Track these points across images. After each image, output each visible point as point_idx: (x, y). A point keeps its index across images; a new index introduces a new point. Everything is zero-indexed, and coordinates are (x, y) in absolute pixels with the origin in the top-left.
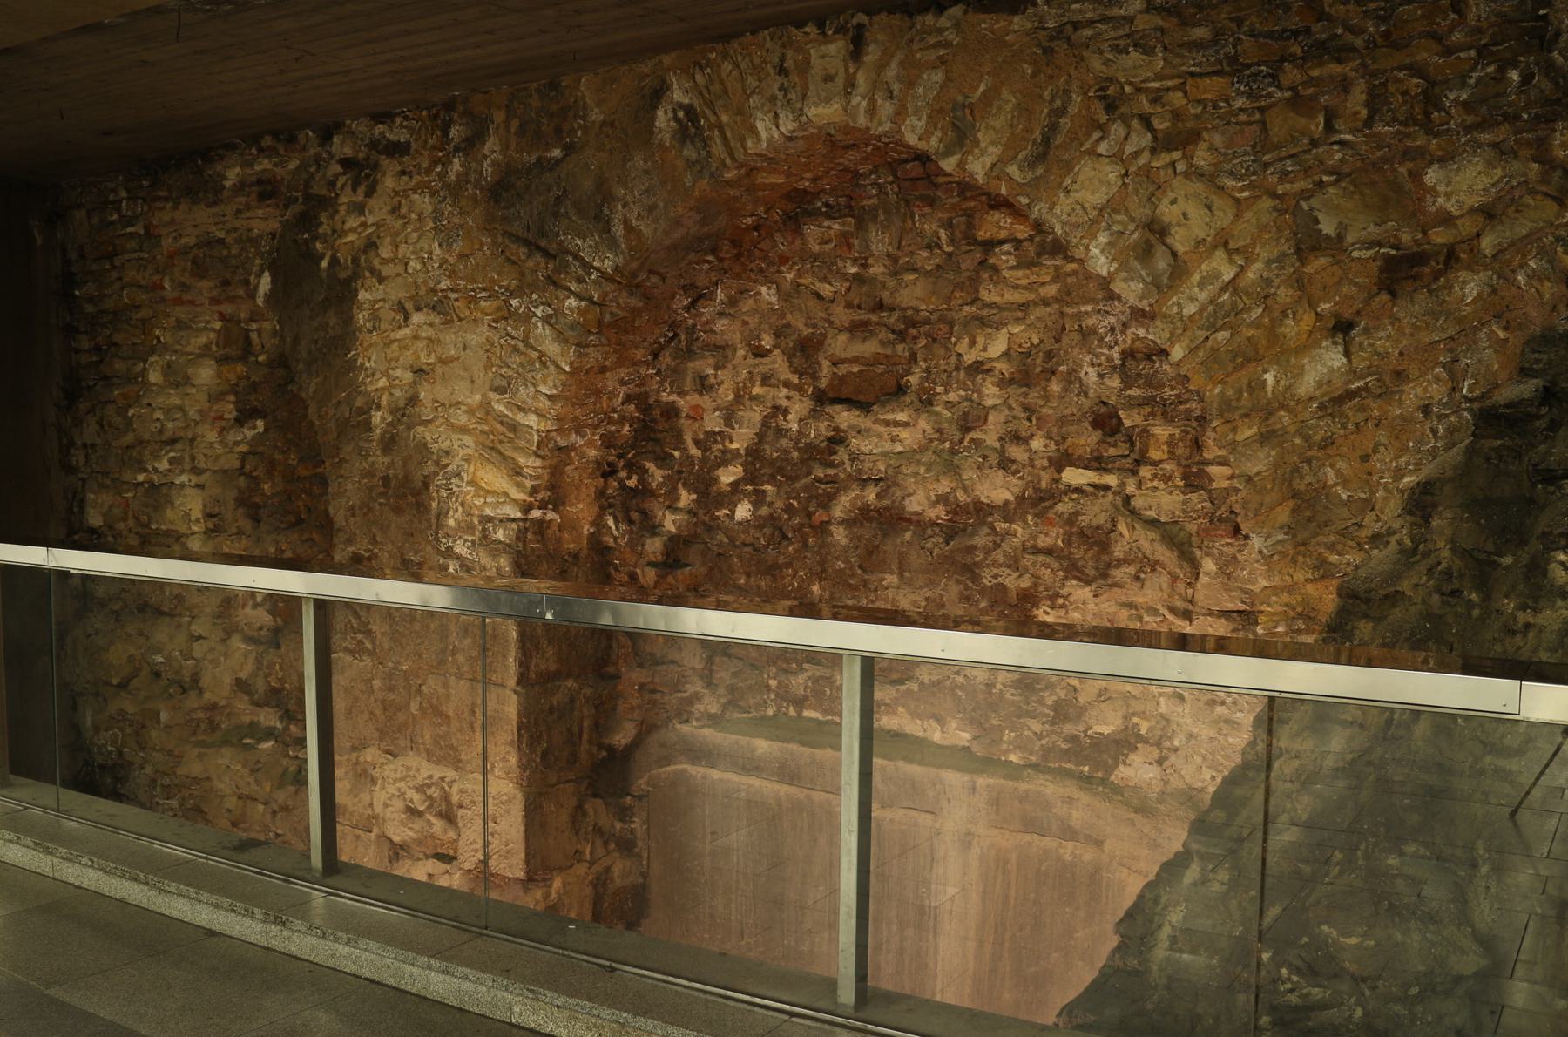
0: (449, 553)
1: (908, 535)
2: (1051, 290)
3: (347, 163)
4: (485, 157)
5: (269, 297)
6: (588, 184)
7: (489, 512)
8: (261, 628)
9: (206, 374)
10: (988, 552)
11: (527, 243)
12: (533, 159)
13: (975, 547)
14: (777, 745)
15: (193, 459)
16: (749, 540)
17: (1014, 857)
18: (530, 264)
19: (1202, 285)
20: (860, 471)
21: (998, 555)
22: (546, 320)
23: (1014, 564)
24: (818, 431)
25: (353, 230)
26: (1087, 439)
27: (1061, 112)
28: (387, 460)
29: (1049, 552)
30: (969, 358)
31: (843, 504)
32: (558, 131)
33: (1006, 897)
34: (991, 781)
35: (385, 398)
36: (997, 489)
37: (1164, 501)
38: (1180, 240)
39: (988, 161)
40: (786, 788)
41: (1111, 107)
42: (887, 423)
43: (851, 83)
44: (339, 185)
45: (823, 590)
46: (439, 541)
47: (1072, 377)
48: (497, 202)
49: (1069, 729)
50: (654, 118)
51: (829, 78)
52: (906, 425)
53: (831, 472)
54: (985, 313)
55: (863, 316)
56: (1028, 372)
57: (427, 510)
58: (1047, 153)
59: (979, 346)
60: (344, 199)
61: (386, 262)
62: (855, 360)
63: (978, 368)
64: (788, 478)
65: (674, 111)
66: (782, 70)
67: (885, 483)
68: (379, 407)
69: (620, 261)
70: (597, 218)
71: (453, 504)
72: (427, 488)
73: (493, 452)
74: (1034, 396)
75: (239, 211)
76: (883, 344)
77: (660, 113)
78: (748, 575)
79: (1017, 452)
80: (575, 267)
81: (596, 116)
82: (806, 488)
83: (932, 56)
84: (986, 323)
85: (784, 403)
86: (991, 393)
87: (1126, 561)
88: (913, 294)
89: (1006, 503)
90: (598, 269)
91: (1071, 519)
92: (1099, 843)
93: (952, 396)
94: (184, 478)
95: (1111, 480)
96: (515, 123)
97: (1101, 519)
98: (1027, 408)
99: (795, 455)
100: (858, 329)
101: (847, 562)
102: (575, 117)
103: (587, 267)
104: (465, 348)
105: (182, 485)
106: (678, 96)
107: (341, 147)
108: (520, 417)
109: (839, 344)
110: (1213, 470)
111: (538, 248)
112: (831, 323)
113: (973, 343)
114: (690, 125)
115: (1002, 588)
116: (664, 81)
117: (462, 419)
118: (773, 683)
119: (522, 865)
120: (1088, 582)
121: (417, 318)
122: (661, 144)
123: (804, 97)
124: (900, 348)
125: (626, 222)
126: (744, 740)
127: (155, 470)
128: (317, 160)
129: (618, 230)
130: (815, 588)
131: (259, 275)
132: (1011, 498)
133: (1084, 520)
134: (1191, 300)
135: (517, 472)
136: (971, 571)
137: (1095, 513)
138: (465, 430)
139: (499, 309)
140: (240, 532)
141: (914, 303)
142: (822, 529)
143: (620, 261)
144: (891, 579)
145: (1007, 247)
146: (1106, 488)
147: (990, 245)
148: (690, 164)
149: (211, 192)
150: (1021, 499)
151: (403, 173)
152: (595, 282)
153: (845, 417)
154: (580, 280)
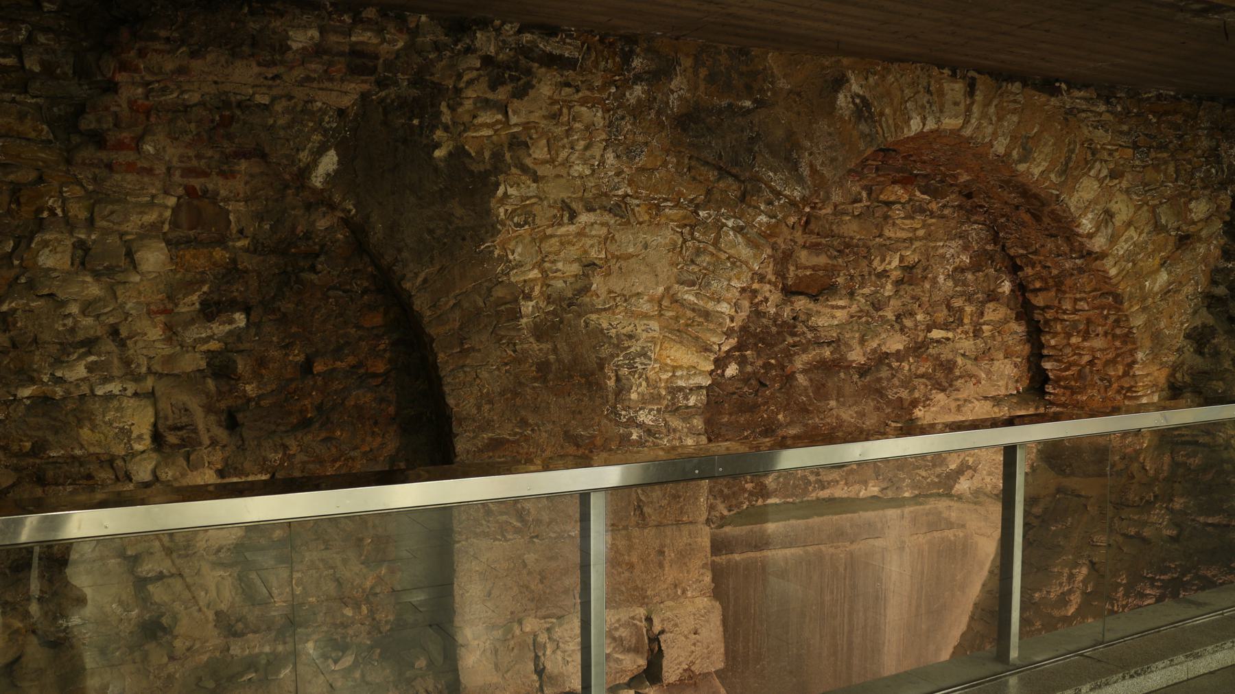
0: (632, 422)
1: (842, 375)
2: (921, 233)
3: (487, 61)
4: (672, 92)
5: (330, 178)
6: (780, 133)
7: (681, 383)
8: (219, 550)
9: (153, 258)
10: (889, 380)
11: (720, 169)
12: (724, 103)
13: (881, 378)
14: (781, 524)
15: (127, 363)
16: (731, 389)
17: (926, 547)
18: (721, 185)
19: (1126, 241)
20: (818, 337)
21: (895, 381)
22: (739, 230)
23: (906, 384)
24: (787, 313)
25: (488, 126)
26: (942, 315)
27: (1072, 151)
28: (546, 346)
29: (922, 376)
30: (880, 269)
31: (800, 362)
32: (748, 87)
33: (923, 573)
34: (912, 509)
35: (537, 289)
36: (896, 343)
37: (967, 345)
38: (1119, 220)
39: (1041, 169)
40: (788, 552)
41: (1093, 154)
42: (833, 307)
43: (968, 110)
44: (465, 78)
45: (785, 417)
46: (618, 414)
47: (934, 281)
48: (684, 130)
49: (938, 470)
50: (836, 98)
51: (956, 104)
52: (843, 308)
53: (797, 339)
54: (888, 242)
55: (814, 239)
56: (910, 275)
57: (601, 387)
58: (1069, 171)
59: (888, 259)
60: (471, 93)
61: (544, 162)
62: (813, 268)
63: (884, 274)
64: (767, 345)
65: (852, 97)
66: (929, 92)
67: (835, 343)
68: (528, 297)
69: (807, 193)
70: (787, 159)
71: (634, 380)
72: (602, 368)
73: (679, 333)
74: (918, 291)
75: (308, 79)
76: (830, 257)
77: (841, 96)
78: (731, 414)
79: (908, 323)
80: (767, 194)
81: (783, 84)
82: (781, 351)
83: (1012, 106)
84: (887, 248)
85: (767, 294)
86: (889, 289)
87: (960, 377)
88: (851, 228)
89: (898, 351)
90: (786, 197)
91: (937, 358)
92: (963, 526)
93: (866, 291)
94: (114, 387)
95: (950, 335)
96: (703, 72)
97: (950, 356)
98: (913, 298)
99: (774, 329)
100: (814, 248)
101: (808, 396)
102: (764, 81)
103: (778, 194)
104: (646, 246)
105: (109, 397)
106: (855, 88)
107: (485, 42)
108: (710, 306)
109: (803, 256)
110: (984, 327)
111: (729, 174)
112: (796, 243)
113: (883, 260)
114: (863, 109)
115: (900, 399)
116: (844, 75)
117: (645, 307)
118: (749, 486)
119: (722, 658)
120: (943, 390)
121: (584, 218)
122: (841, 118)
123: (941, 111)
124: (840, 260)
125: (811, 166)
126: (756, 527)
127: (60, 381)
128: (437, 47)
129: (805, 171)
130: (780, 417)
131: (321, 151)
132: (901, 347)
133: (943, 357)
134: (1122, 248)
135: (707, 349)
136: (880, 393)
137: (946, 354)
138: (646, 316)
139: (685, 217)
140: (214, 442)
141: (852, 234)
142: (791, 377)
143: (807, 193)
144: (833, 403)
145: (898, 206)
146: (948, 339)
147: (889, 204)
148: (863, 136)
149: (272, 51)
150: (907, 349)
151: (568, 85)
152: (782, 206)
153: (801, 303)
154: (770, 203)
